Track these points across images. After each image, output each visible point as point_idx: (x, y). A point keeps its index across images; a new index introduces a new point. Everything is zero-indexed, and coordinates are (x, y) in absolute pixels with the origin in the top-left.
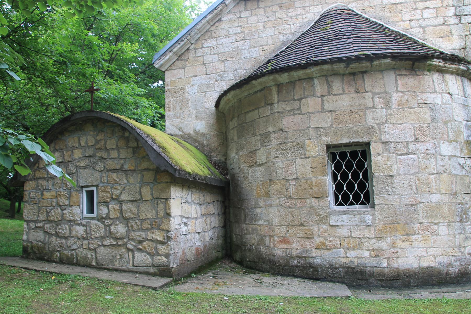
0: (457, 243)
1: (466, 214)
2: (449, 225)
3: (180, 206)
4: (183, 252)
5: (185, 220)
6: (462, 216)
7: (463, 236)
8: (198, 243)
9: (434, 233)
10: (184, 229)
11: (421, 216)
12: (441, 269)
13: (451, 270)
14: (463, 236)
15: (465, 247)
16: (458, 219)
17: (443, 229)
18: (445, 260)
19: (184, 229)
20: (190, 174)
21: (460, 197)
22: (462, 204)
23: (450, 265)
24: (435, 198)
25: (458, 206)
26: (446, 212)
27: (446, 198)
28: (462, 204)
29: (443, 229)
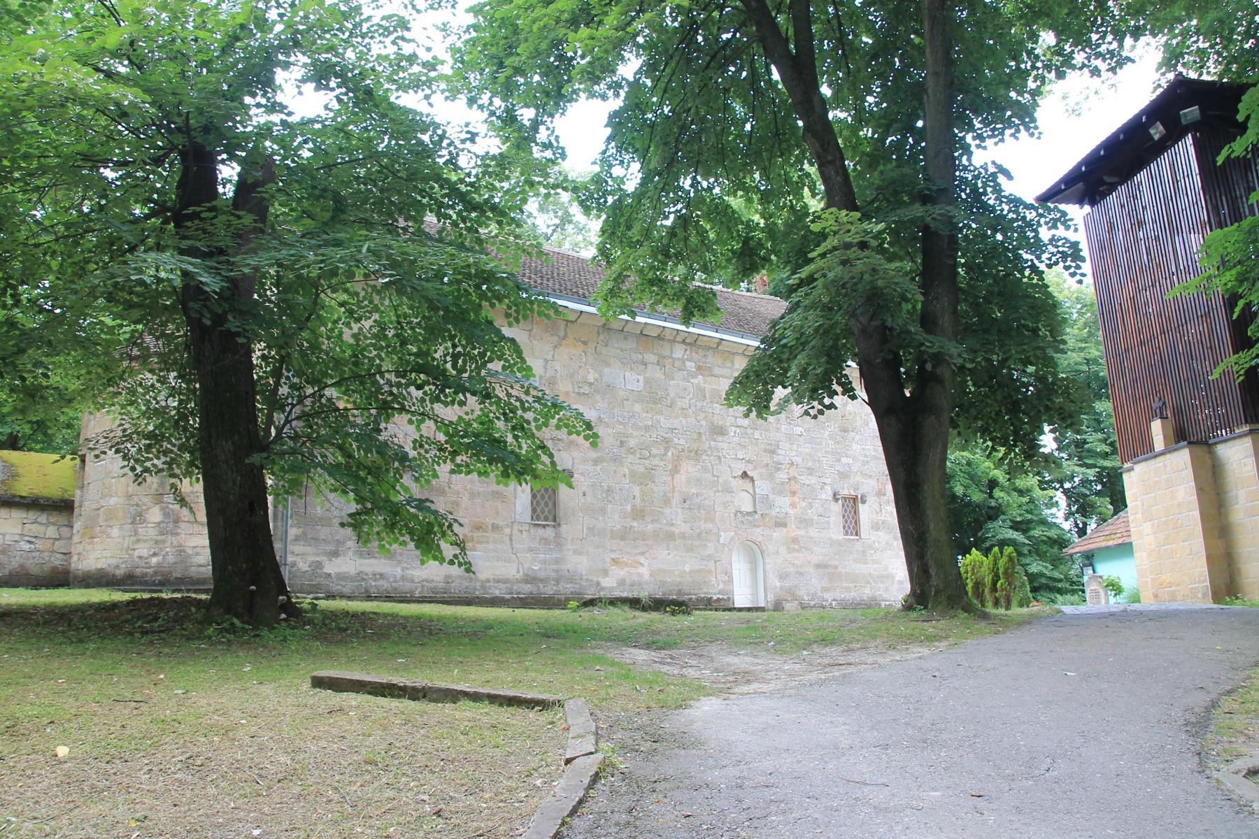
0: (126, 545)
1: (140, 515)
2: (121, 528)
3: (20, 526)
4: (22, 566)
5: (27, 538)
6: (135, 518)
7: (134, 539)
8: (57, 563)
9: (108, 536)
10: (27, 547)
11: (101, 521)
12: (109, 569)
13: (118, 572)
14: (134, 539)
15: (134, 549)
16: (129, 521)
17: (115, 532)
18: (113, 562)
19: (27, 547)
20: (22, 497)
21: (136, 499)
22: (137, 505)
23: (117, 567)
24: (113, 501)
25: (132, 508)
26: (120, 514)
27: (121, 500)
28: (137, 505)
29: (115, 532)
